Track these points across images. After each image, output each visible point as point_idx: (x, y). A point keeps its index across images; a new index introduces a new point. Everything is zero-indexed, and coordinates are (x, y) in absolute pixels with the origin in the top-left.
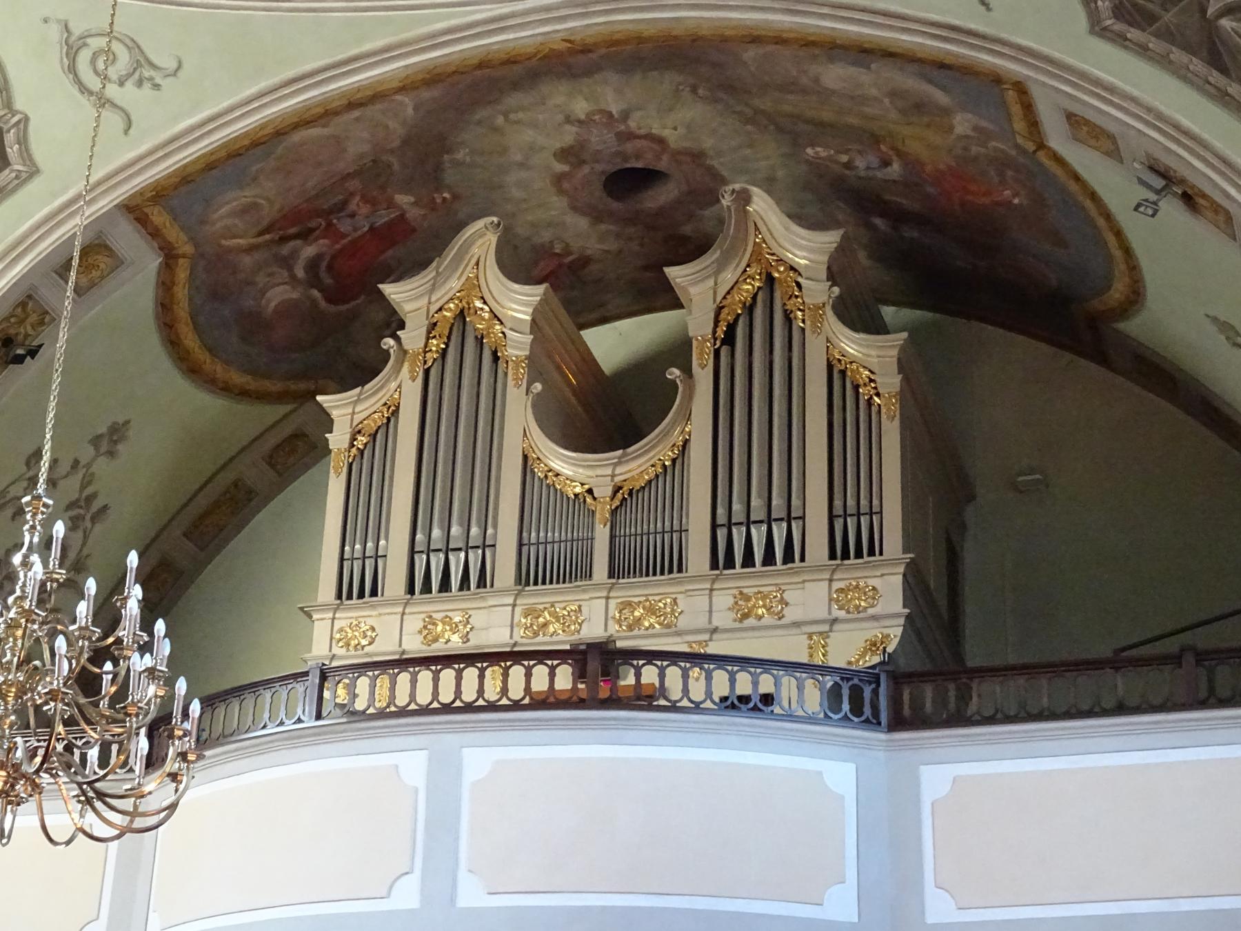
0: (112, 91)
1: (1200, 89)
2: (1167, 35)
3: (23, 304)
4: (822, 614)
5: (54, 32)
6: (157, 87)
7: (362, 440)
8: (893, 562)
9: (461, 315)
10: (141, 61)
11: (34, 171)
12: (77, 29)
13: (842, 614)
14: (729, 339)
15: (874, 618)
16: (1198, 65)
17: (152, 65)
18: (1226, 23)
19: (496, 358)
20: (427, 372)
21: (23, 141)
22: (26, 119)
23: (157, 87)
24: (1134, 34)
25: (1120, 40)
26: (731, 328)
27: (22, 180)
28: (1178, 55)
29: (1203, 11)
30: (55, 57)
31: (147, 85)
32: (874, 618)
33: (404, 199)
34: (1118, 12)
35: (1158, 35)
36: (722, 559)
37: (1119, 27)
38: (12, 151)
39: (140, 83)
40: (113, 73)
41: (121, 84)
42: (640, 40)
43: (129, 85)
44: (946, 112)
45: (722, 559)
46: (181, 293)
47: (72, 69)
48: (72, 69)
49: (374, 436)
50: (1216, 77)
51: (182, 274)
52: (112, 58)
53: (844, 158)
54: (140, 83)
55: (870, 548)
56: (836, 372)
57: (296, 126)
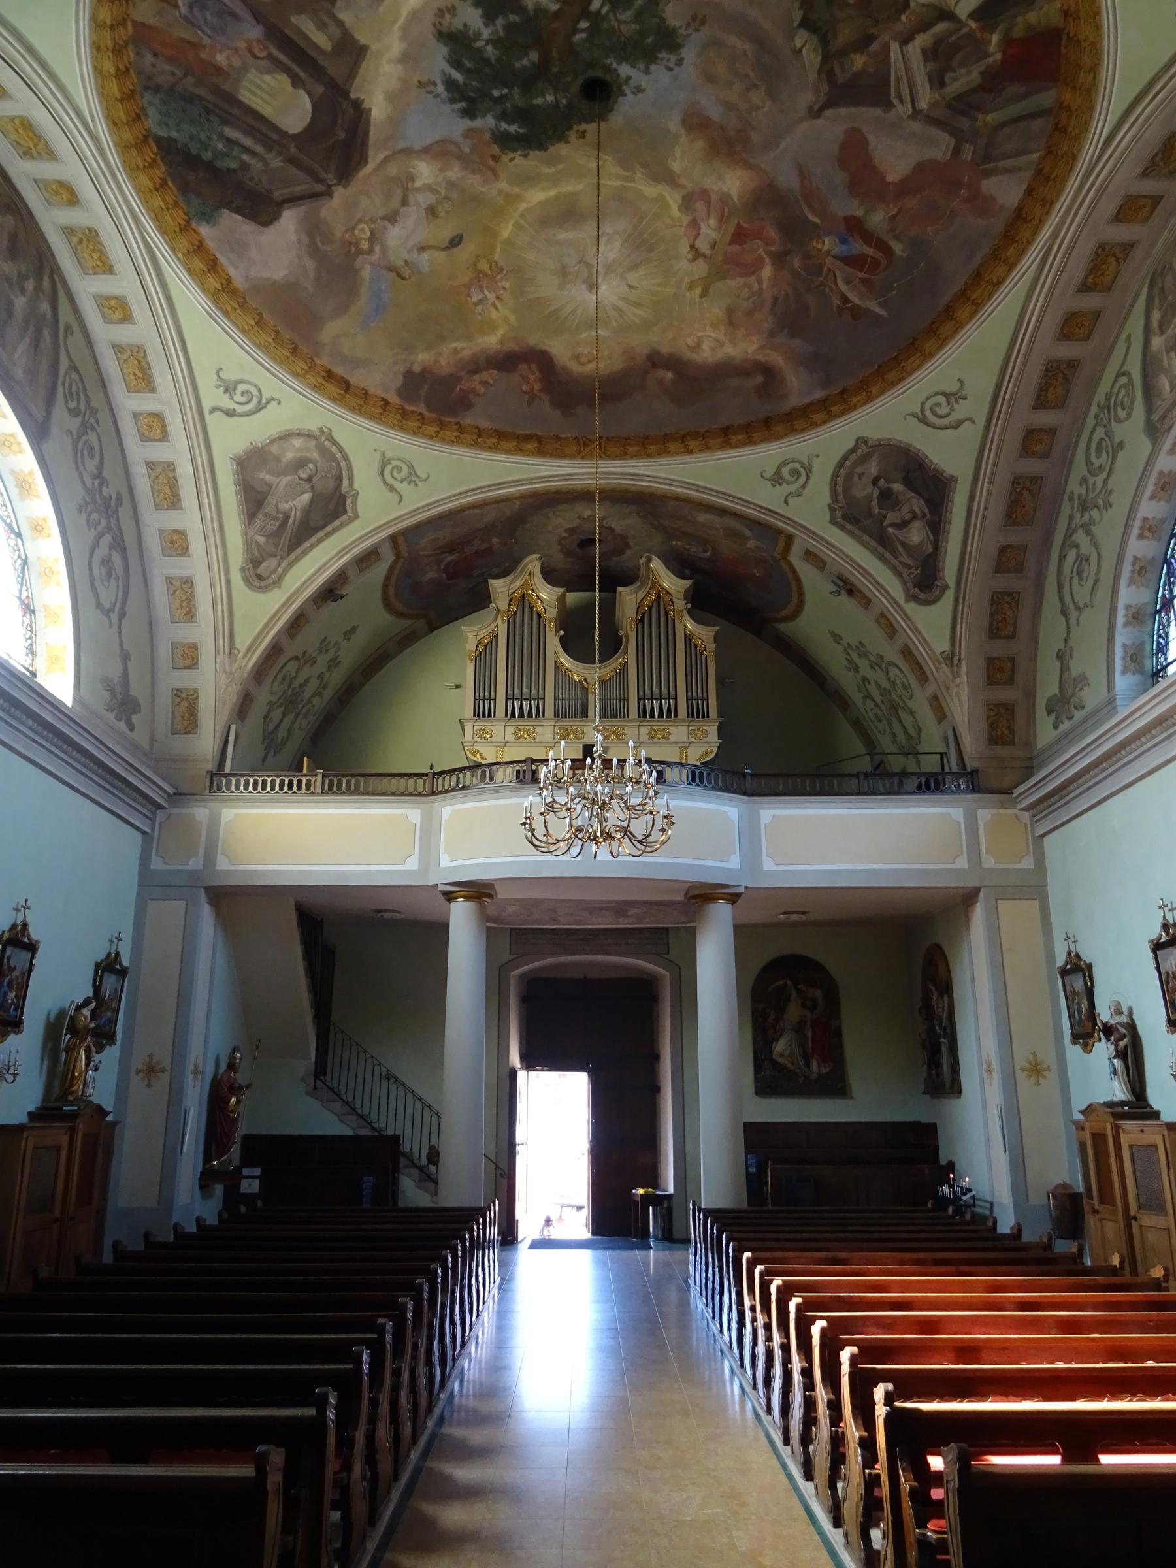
0: (397, 485)
1: (871, 552)
2: (864, 530)
3: (340, 575)
4: (686, 740)
5: (378, 456)
6: (416, 485)
7: (481, 647)
8: (713, 721)
9: (523, 596)
10: (412, 472)
11: (356, 517)
12: (389, 455)
13: (693, 740)
14: (642, 620)
15: (707, 743)
16: (873, 543)
17: (417, 475)
18: (890, 530)
19: (539, 616)
20: (509, 620)
21: (354, 503)
22: (358, 493)
23: (416, 485)
24: (849, 526)
25: (842, 527)
26: (643, 615)
27: (351, 520)
28: (866, 538)
29: (882, 522)
30: (376, 466)
31: (412, 484)
32: (707, 743)
33: (495, 541)
34: (845, 517)
35: (859, 529)
36: (642, 714)
37: (843, 523)
38: (349, 506)
39: (409, 483)
40: (399, 477)
41: (402, 482)
42: (627, 491)
43: (405, 483)
44: (747, 539)
45: (642, 714)
46: (396, 571)
47: (382, 473)
48: (382, 473)
49: (486, 646)
50: (880, 549)
51: (399, 564)
52: (400, 470)
53: (688, 547)
54: (409, 483)
55: (705, 715)
56: (688, 639)
57: (469, 508)
